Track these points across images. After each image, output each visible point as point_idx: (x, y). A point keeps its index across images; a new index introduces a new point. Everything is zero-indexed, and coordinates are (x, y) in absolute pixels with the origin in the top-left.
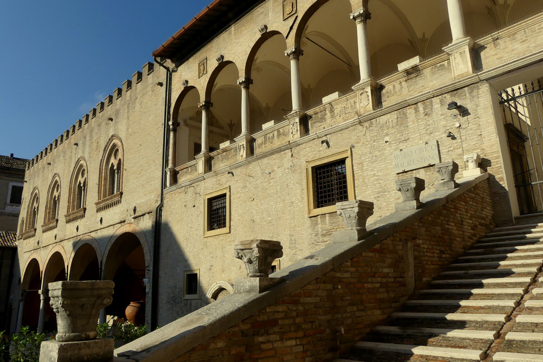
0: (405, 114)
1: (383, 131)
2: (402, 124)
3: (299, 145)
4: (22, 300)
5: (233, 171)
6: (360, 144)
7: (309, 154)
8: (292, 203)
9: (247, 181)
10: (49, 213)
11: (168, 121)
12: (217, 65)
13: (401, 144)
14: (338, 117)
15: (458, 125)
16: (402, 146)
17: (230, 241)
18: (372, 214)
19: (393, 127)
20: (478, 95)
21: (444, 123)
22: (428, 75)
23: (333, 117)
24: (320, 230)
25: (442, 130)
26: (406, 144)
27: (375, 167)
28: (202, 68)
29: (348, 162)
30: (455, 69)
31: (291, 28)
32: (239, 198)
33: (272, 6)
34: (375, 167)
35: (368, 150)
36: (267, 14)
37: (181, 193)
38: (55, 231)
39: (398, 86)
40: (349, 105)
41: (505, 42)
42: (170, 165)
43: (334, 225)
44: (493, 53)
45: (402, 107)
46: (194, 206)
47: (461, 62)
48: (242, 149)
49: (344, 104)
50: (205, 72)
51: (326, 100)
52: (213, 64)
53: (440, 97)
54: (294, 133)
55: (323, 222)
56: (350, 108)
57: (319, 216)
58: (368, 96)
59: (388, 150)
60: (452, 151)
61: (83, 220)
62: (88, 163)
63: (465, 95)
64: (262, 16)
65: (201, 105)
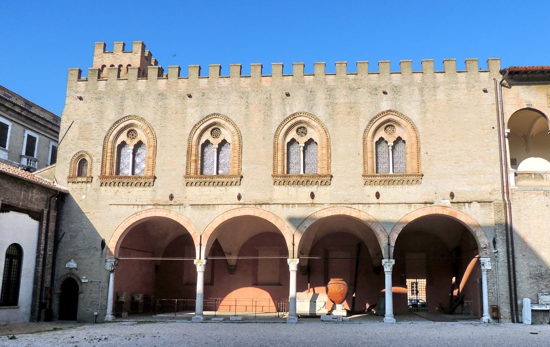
4: (112, 271)
10: (196, 161)
37: (539, 194)
38: (235, 190)
61: (328, 188)
62: (328, 125)
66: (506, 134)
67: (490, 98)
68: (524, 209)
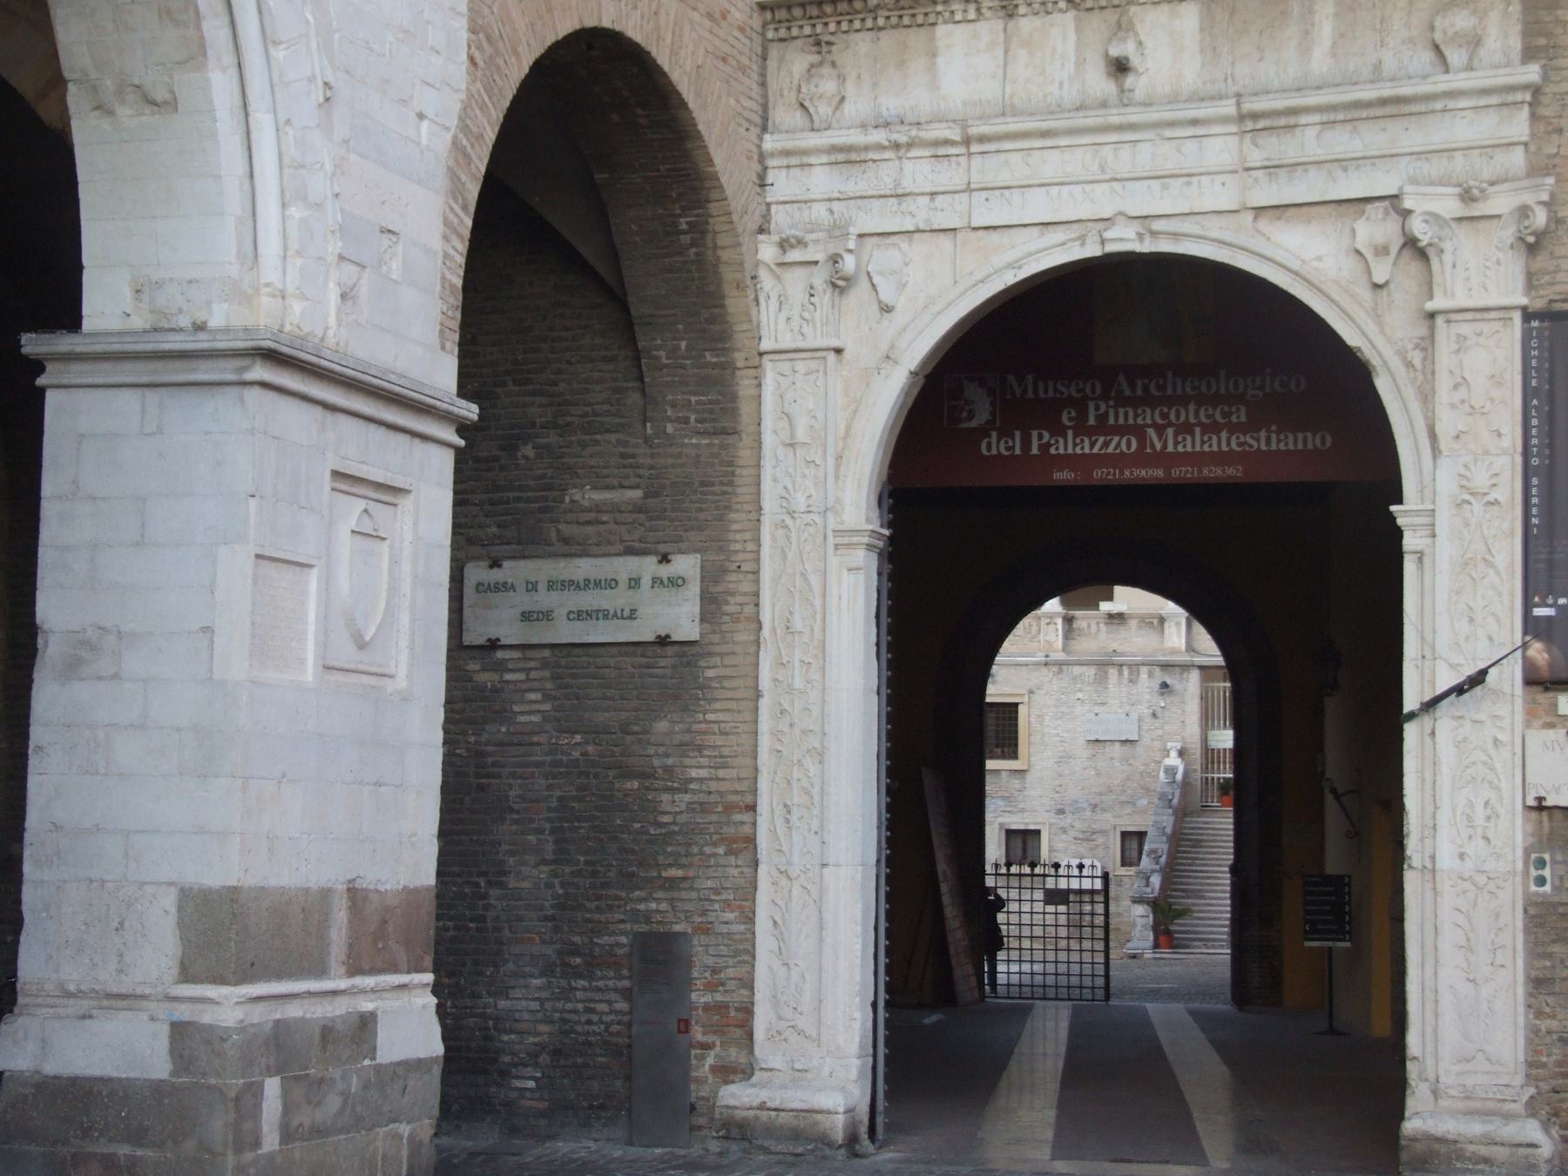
39: (1094, 626)
45: (1105, 664)
59: (1079, 709)
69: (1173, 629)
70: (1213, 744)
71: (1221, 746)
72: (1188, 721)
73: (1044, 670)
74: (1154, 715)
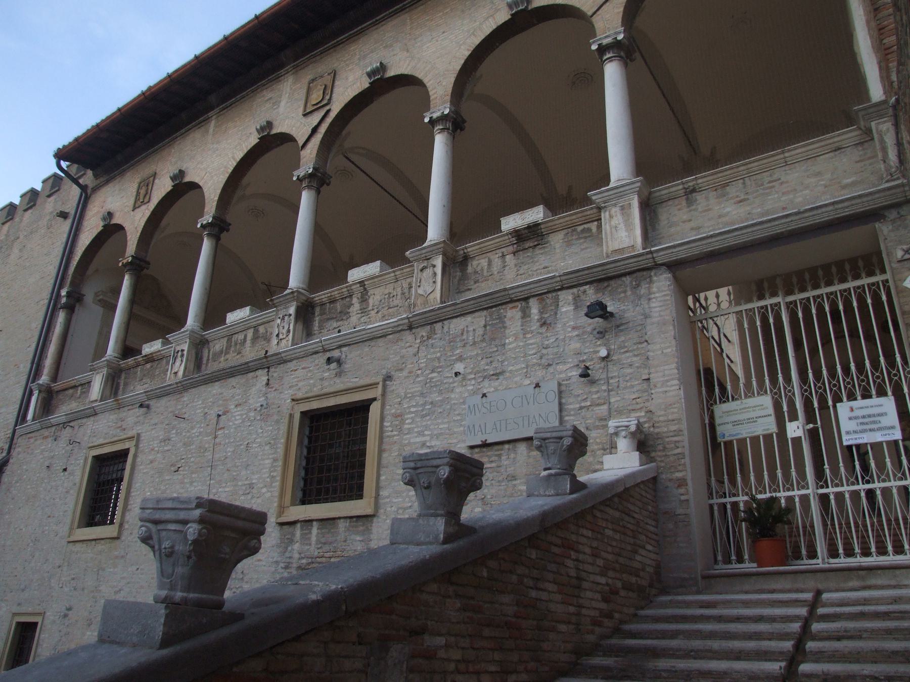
0: (501, 319)
1: (453, 349)
2: (493, 339)
3: (285, 362)
5: (151, 403)
6: (405, 373)
7: (300, 384)
8: (251, 486)
9: (173, 428)
11: (61, 287)
12: (170, 188)
13: (486, 383)
14: (373, 313)
15: (603, 353)
16: (488, 387)
17: (117, 557)
18: (255, 550)
19: (474, 343)
20: (650, 293)
21: (578, 345)
22: (557, 246)
23: (364, 311)
24: (296, 556)
25: (572, 361)
26: (496, 383)
27: (427, 427)
28: (142, 192)
29: (375, 409)
30: (609, 237)
31: (315, 130)
32: (151, 462)
33: (288, 89)
34: (427, 427)
35: (417, 388)
36: (277, 103)
37: (46, 437)
39: (497, 262)
40: (399, 289)
41: (707, 198)
42: (44, 379)
43: (326, 548)
44: (685, 217)
45: (497, 303)
46: (65, 470)
47: (622, 226)
48: (179, 359)
49: (389, 289)
50: (146, 200)
51: (355, 275)
52: (163, 187)
53: (575, 290)
54: (281, 336)
55: (305, 538)
56: (399, 297)
57: (299, 525)
58: (435, 274)
60: (588, 407)
63: (625, 292)
64: (268, 105)
65: (125, 261)
66: (64, 300)
67: (65, 226)
68: (17, 482)
69: (618, 219)
70: (727, 431)
71: (745, 432)
72: (656, 378)
73: (408, 337)
74: (585, 375)
